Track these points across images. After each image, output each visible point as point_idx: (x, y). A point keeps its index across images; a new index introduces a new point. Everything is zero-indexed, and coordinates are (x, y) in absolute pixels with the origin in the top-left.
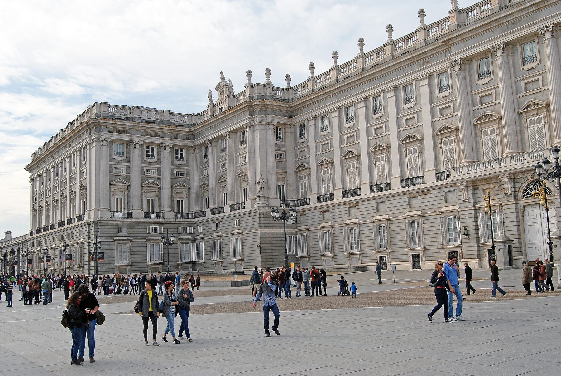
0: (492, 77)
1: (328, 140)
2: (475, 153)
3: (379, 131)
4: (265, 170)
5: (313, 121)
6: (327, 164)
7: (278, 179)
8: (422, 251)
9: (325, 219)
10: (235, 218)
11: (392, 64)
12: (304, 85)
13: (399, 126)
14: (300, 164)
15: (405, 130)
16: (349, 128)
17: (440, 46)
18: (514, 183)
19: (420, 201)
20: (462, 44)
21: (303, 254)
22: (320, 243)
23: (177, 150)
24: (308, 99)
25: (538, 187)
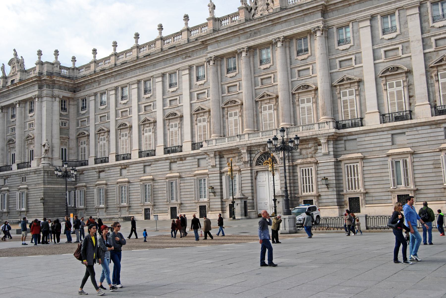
0: (237, 72)
1: (105, 113)
2: (222, 129)
3: (148, 108)
4: (50, 135)
5: (94, 96)
6: (104, 132)
7: (62, 143)
8: (179, 205)
9: (101, 177)
10: (22, 175)
11: (161, 55)
12: (87, 66)
13: (164, 105)
14: (80, 131)
15: (169, 109)
16: (123, 104)
17: (199, 45)
18: (250, 154)
19: (178, 165)
20: (216, 45)
21: (81, 206)
22: (96, 197)
24: (90, 78)
25: (268, 157)
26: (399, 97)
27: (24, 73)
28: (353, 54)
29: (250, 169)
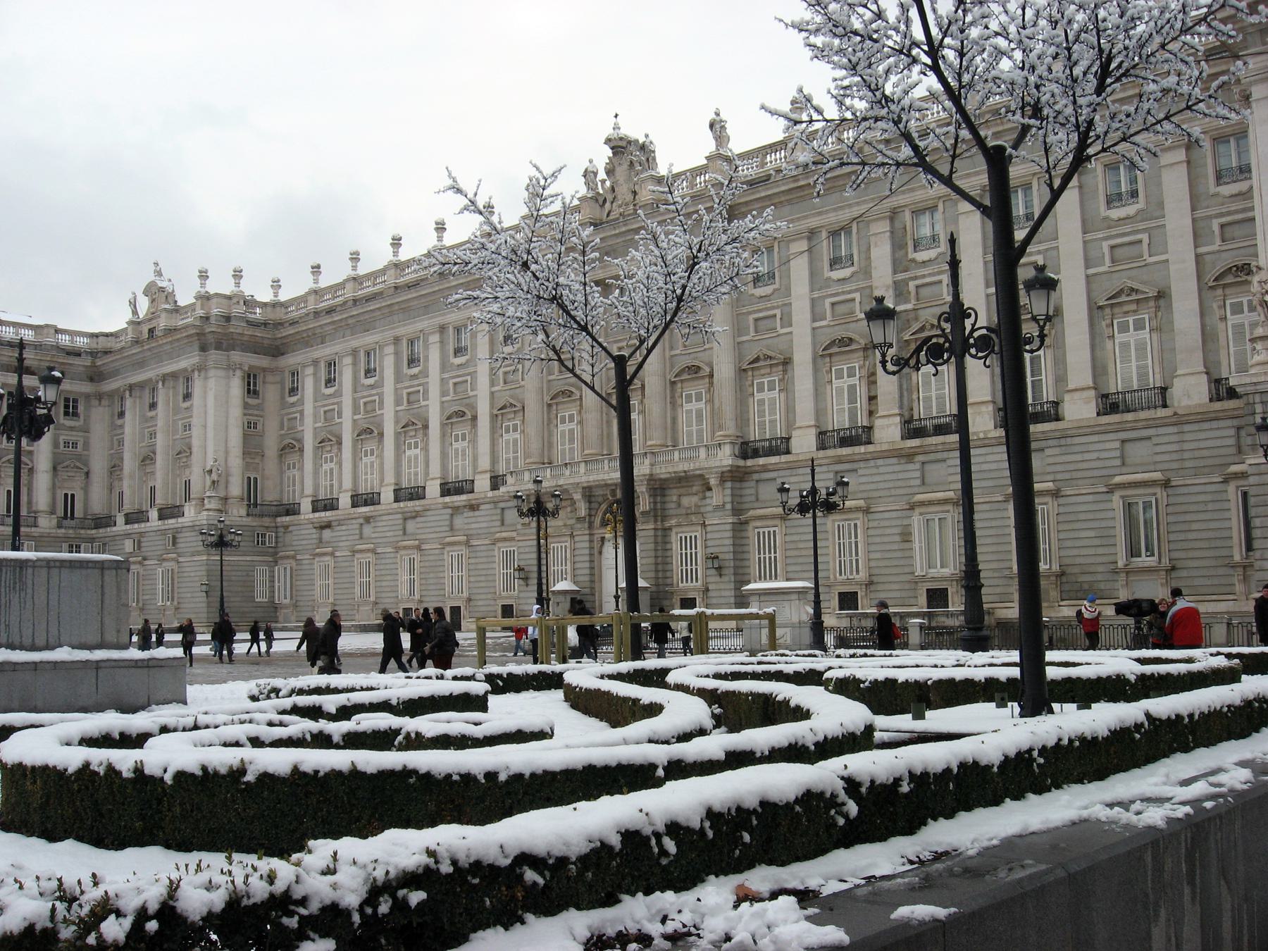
2: (546, 448)
7: (247, 466)
12: (303, 299)
14: (286, 442)
18: (590, 502)
19: (466, 521)
23: (67, 400)
26: (852, 400)
27: (174, 314)
28: (777, 307)
29: (587, 532)
